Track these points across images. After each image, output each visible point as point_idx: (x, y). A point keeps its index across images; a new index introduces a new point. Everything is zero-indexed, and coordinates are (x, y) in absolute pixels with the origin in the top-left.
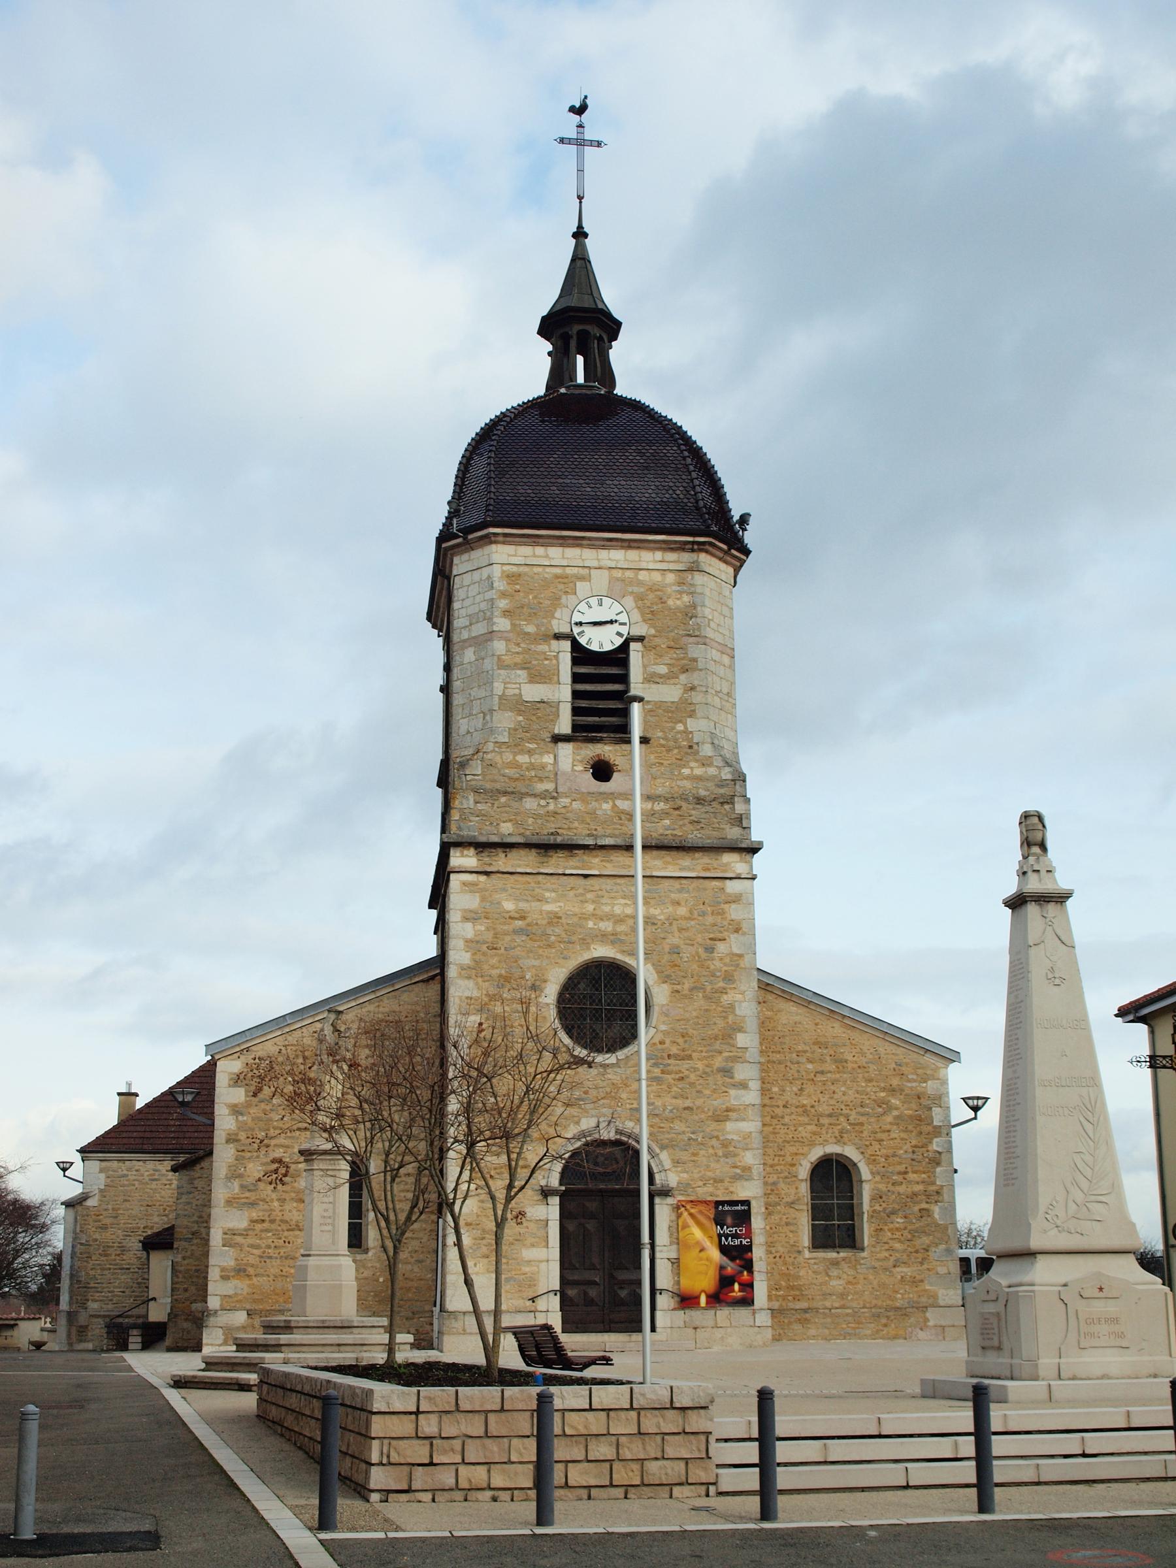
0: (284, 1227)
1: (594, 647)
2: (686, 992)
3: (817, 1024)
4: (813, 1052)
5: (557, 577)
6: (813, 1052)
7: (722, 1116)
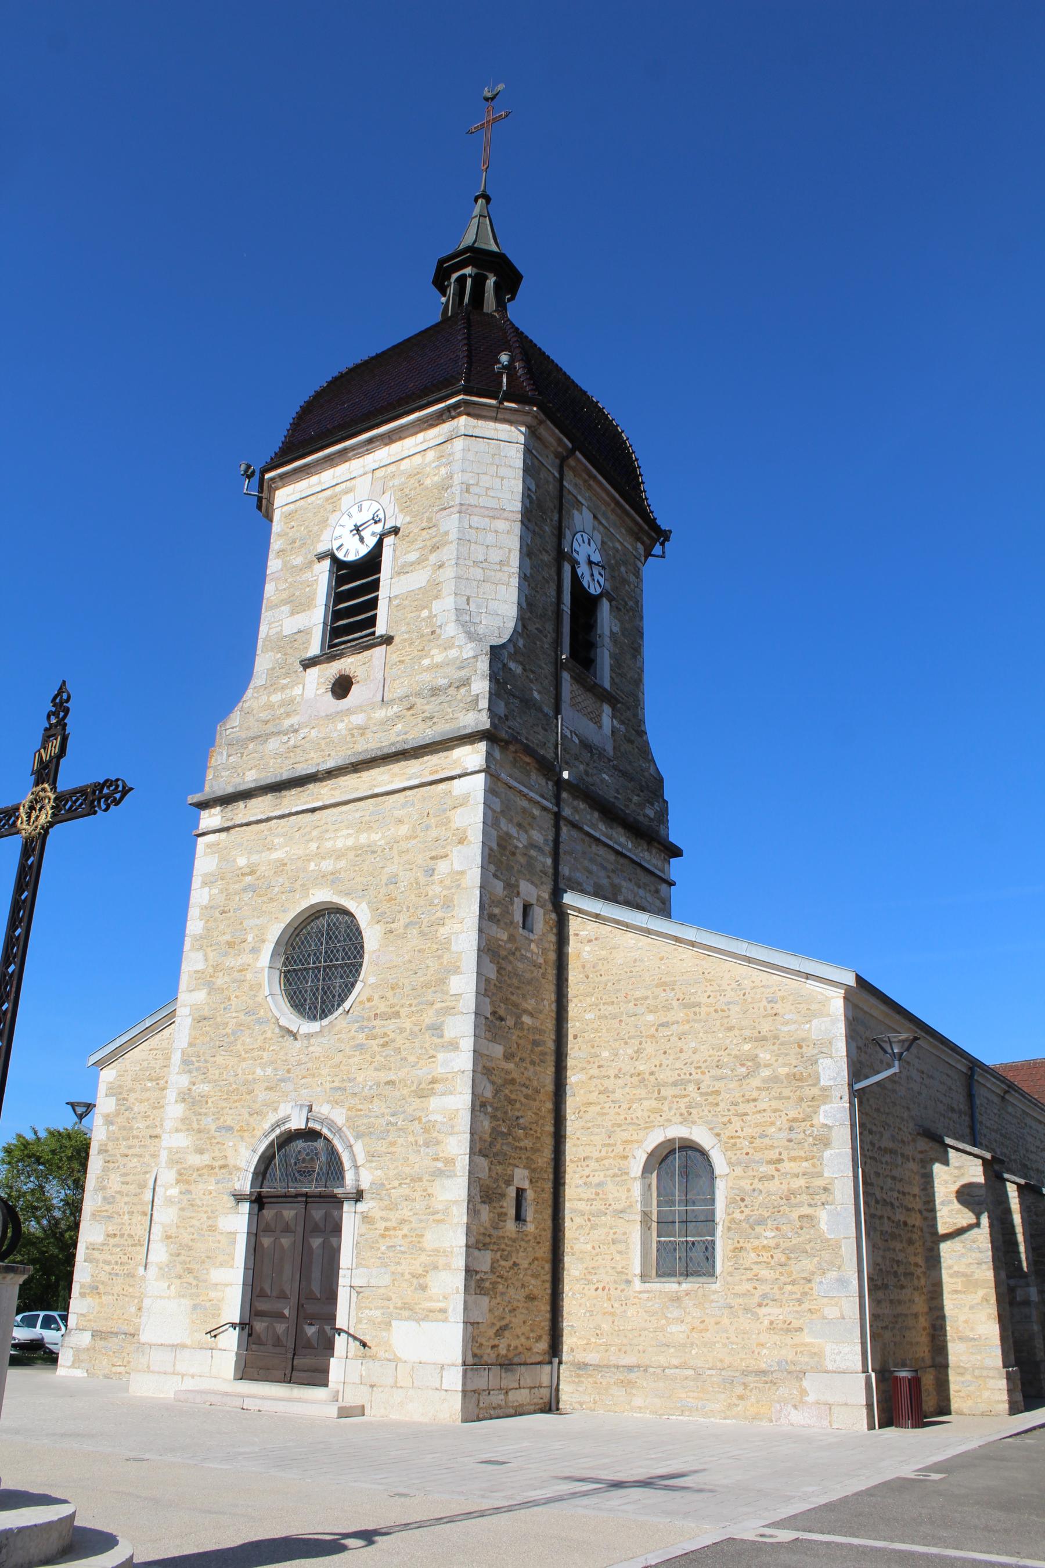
0: (130, 1242)
1: (351, 557)
2: (401, 931)
3: (662, 959)
4: (655, 998)
5: (327, 499)
6: (655, 998)
7: (425, 1091)
